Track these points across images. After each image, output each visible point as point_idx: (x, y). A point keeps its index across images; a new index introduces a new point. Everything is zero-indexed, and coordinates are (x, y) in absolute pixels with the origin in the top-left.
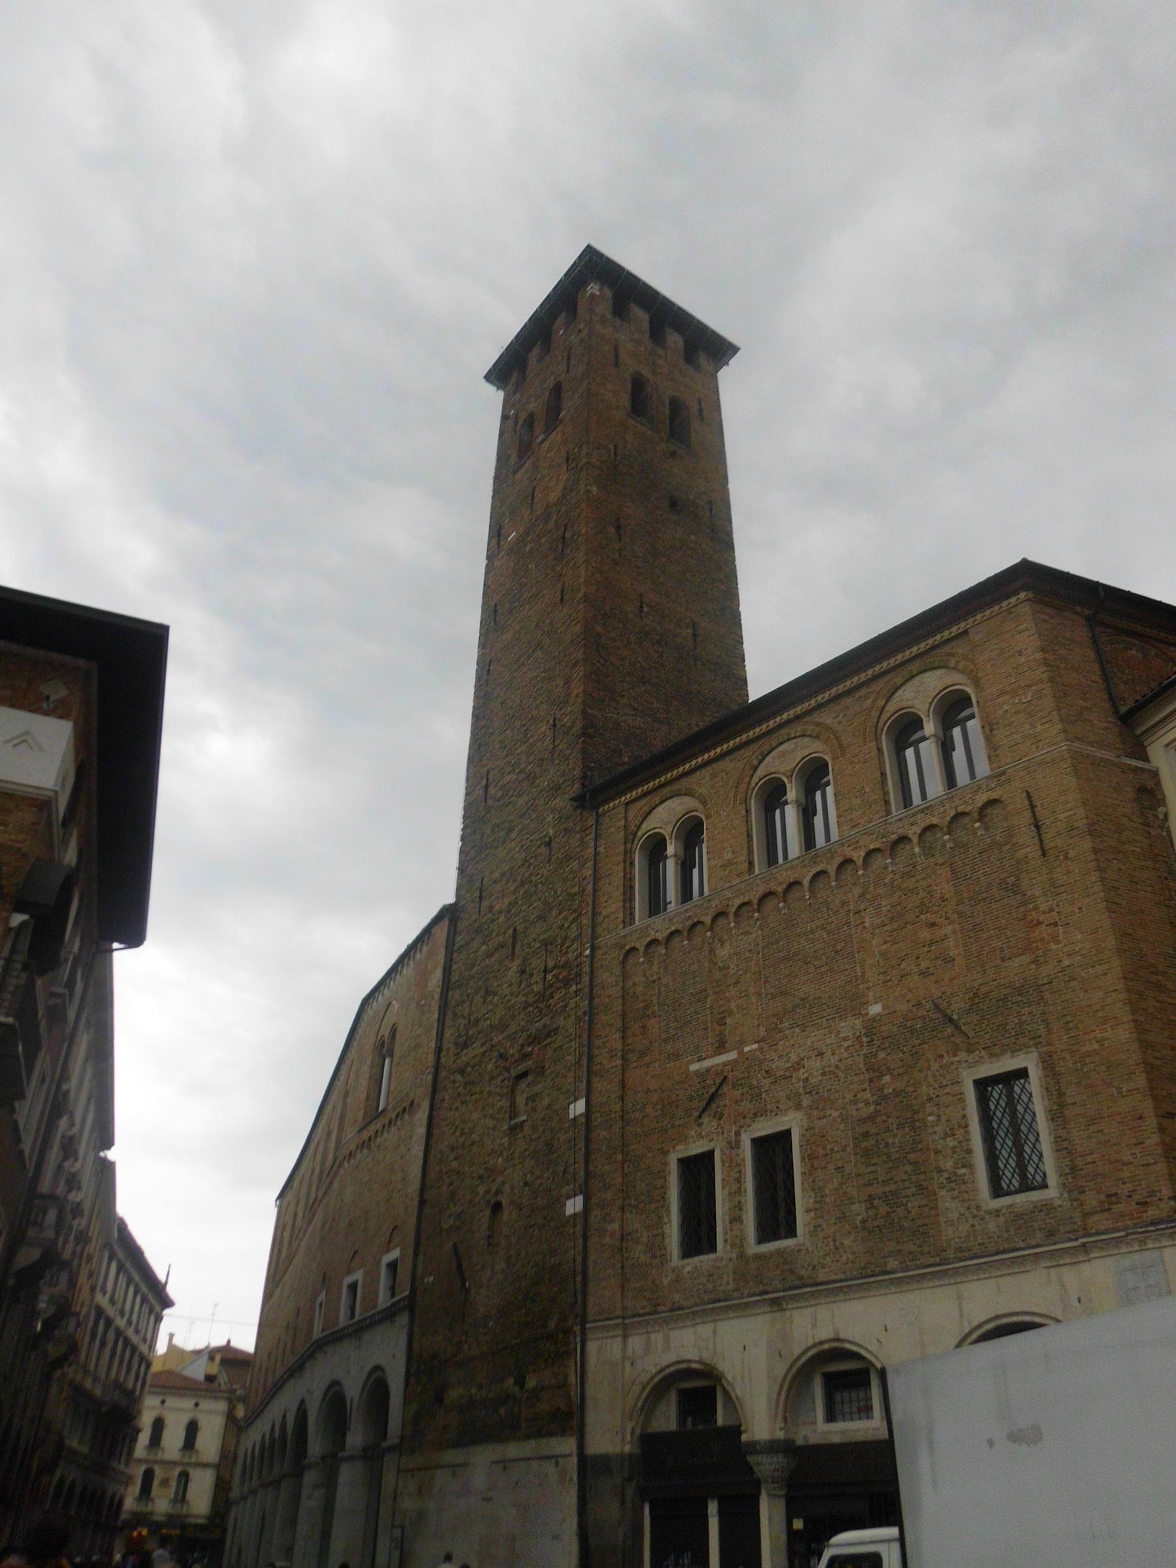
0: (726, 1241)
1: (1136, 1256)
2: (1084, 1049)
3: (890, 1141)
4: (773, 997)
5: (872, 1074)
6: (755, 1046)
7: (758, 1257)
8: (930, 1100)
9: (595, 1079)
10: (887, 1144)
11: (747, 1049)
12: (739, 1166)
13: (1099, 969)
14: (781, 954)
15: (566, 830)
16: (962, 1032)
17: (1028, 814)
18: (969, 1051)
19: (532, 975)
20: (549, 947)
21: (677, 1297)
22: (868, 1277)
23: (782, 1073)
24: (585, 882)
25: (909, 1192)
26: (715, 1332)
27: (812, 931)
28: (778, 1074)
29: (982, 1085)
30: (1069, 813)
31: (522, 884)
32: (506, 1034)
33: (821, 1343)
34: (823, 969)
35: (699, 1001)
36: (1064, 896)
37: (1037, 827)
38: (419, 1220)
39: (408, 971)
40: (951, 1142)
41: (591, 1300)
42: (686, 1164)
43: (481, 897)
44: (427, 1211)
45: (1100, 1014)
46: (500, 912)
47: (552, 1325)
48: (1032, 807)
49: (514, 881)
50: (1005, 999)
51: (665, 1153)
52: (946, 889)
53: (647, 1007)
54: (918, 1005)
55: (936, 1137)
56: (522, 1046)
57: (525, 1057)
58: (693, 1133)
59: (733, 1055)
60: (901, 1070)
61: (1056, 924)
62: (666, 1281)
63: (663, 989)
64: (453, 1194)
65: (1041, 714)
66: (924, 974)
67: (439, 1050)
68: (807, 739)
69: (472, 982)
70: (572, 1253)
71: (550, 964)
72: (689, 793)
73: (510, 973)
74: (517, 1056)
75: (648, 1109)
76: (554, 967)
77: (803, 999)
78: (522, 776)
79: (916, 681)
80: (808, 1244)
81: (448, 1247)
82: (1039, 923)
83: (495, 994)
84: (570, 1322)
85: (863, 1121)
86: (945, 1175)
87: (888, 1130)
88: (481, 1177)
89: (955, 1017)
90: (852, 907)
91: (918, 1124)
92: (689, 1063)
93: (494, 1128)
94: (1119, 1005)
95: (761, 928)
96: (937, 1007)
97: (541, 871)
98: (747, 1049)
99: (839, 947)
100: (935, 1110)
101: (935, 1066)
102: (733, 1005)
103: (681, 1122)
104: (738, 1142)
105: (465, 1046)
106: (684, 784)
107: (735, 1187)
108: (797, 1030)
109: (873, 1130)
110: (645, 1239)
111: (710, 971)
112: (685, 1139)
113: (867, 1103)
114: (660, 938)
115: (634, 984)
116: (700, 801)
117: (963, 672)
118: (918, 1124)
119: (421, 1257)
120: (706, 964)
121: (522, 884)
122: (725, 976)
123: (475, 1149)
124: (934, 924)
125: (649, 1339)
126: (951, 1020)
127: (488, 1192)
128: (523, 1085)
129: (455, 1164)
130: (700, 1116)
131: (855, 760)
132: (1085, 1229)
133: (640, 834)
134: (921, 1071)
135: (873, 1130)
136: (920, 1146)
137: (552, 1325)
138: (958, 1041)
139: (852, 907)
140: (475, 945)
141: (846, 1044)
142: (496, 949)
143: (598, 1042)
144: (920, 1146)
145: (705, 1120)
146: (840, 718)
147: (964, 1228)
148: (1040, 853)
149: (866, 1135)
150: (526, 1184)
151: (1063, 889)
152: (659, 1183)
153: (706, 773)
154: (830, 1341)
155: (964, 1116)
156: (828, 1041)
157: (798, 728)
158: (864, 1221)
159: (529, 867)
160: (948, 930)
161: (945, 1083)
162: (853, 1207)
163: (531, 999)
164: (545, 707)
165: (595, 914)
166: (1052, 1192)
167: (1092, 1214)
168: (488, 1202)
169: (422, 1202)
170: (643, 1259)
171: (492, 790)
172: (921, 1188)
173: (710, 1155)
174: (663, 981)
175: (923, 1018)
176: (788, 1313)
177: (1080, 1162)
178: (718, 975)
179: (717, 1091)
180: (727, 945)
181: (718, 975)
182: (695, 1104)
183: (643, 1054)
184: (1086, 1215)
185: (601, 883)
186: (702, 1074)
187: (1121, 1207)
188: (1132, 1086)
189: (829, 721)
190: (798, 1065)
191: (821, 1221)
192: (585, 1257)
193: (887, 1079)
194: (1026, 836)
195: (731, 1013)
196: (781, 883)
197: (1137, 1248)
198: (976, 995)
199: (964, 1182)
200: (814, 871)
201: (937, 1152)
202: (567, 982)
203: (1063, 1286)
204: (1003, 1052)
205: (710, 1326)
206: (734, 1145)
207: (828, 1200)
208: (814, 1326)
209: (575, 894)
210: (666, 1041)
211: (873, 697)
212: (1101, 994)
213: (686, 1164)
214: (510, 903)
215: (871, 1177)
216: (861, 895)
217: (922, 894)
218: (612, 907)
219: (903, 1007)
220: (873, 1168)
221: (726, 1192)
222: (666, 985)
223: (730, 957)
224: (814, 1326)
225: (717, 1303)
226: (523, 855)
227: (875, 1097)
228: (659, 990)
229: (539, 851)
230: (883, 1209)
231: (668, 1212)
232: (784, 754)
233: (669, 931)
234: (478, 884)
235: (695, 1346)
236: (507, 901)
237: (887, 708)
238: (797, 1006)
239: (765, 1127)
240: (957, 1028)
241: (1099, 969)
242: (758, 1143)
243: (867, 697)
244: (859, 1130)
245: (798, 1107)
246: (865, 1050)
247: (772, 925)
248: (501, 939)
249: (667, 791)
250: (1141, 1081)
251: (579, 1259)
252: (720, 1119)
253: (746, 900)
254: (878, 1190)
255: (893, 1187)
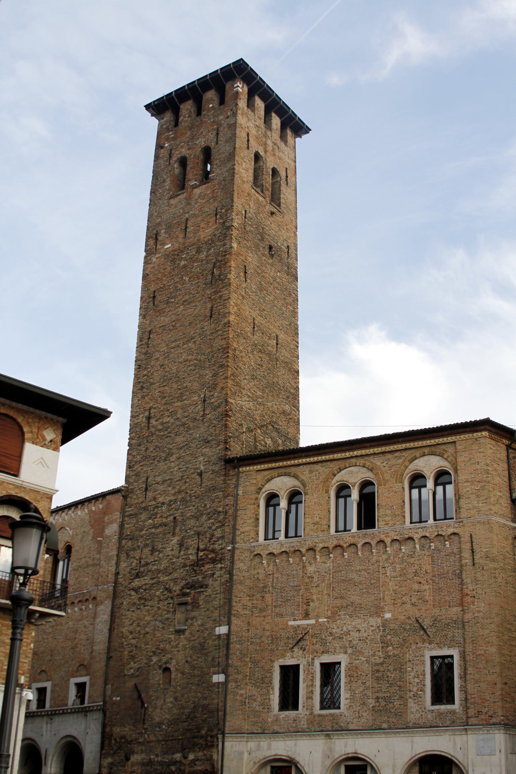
0: (304, 707)
1: (485, 735)
2: (478, 653)
3: (389, 675)
4: (336, 598)
5: (383, 645)
6: (325, 620)
7: (320, 715)
8: (410, 661)
9: (233, 618)
10: (388, 677)
11: (320, 620)
12: (313, 674)
13: (489, 621)
14: (343, 578)
15: (213, 471)
16: (428, 635)
17: (469, 545)
18: (430, 644)
19: (187, 549)
20: (201, 537)
21: (276, 728)
22: (373, 729)
23: (338, 635)
24: (227, 508)
25: (395, 698)
26: (295, 745)
27: (359, 571)
28: (336, 635)
29: (432, 658)
30: (487, 550)
31: (180, 492)
32: (170, 577)
33: (348, 754)
34: (364, 591)
35: (296, 590)
36: (480, 586)
37: (473, 552)
38: (107, 666)
39: (81, 513)
40: (417, 680)
41: (227, 724)
42: (284, 669)
43: (146, 490)
44: (112, 663)
45: (487, 640)
46: (163, 503)
47: (203, 732)
48: (472, 542)
49: (174, 488)
50: (448, 624)
51: (273, 661)
52: (429, 568)
53: (265, 587)
54: (409, 618)
55: (410, 677)
56: (183, 588)
57: (185, 595)
58: (288, 654)
59: (313, 622)
60: (398, 646)
61: (474, 597)
62: (269, 720)
63: (275, 580)
64: (133, 657)
65: (483, 498)
66: (413, 605)
67: (117, 574)
68: (365, 469)
69: (141, 540)
70: (216, 701)
71: (202, 547)
72: (296, 477)
73: (172, 543)
74: (178, 592)
75: (264, 639)
76: (205, 549)
77: (352, 603)
78: (178, 423)
79: (426, 458)
80: (346, 713)
81: (130, 684)
82: (467, 595)
83: (160, 552)
84: (215, 732)
85: (377, 664)
86: (413, 693)
87: (388, 670)
88: (154, 652)
89: (425, 627)
90: (381, 564)
91: (403, 670)
92: (288, 620)
93: (163, 628)
94: (495, 637)
95: (333, 562)
96: (417, 621)
97: (195, 489)
98: (320, 620)
99: (373, 582)
100: (411, 666)
101: (414, 647)
102: (314, 597)
103: (282, 648)
104: (313, 663)
105: (137, 576)
106: (293, 470)
107: (310, 683)
108: (348, 617)
109: (382, 669)
110: (259, 699)
111: (303, 577)
112: (283, 656)
113: (380, 657)
114: (275, 553)
115: (258, 573)
116: (302, 484)
117: (450, 463)
118: (403, 670)
119: (109, 686)
120: (301, 573)
121: (180, 492)
122: (311, 581)
123: (148, 636)
124: (420, 583)
125: (259, 745)
126: (423, 629)
127: (160, 661)
128: (183, 608)
129: (134, 641)
130: (293, 648)
131: (391, 490)
132: (467, 722)
133: (264, 490)
134: (407, 648)
135: (382, 669)
136: (403, 680)
137: (203, 732)
138: (425, 638)
139: (381, 564)
140: (143, 517)
141: (372, 628)
142: (160, 525)
143: (234, 599)
144: (403, 680)
145: (296, 649)
146: (384, 464)
147: (418, 715)
148: (472, 563)
149: (378, 671)
150: (187, 662)
151: (479, 582)
152: (268, 675)
153: (307, 468)
154: (353, 753)
155: (424, 671)
156: (363, 625)
157: (361, 461)
158: (373, 707)
159: (186, 483)
160: (426, 587)
161: (417, 655)
162: (369, 700)
163: (188, 562)
164: (196, 384)
165: (234, 528)
166: (457, 706)
167: (471, 717)
168: (160, 667)
169: (109, 658)
170: (258, 708)
171: (153, 422)
172: (401, 697)
173: (298, 666)
174: (275, 576)
175: (410, 624)
176: (333, 740)
177: (469, 697)
178: (307, 580)
179: (303, 637)
180: (314, 565)
181: (307, 580)
182: (291, 641)
183: (261, 610)
184: (468, 718)
185: (239, 512)
186: (295, 627)
187: (482, 717)
188: (494, 671)
189: (379, 464)
190: (348, 633)
191: (353, 704)
192: (225, 705)
193: (390, 648)
194: (466, 554)
195: (313, 601)
196: (346, 543)
197: (486, 732)
198: (435, 620)
199: (420, 697)
200: (364, 541)
201: (410, 683)
202: (214, 561)
203: (455, 742)
204: (445, 645)
205: (294, 742)
206: (311, 664)
207: (357, 695)
208: (345, 747)
209: (220, 512)
210: (275, 607)
211: (403, 458)
212: (488, 632)
213: (284, 669)
214: (171, 501)
215: (379, 689)
216: (387, 560)
217: (416, 567)
218: (244, 526)
219: (402, 618)
220: (380, 685)
221: (305, 684)
222: (277, 578)
223: (315, 572)
224: (345, 747)
225: (296, 731)
226: (180, 474)
227: (384, 656)
228: (273, 580)
229: (193, 476)
230: (383, 703)
231: (273, 689)
232: (352, 472)
233: (281, 551)
234: (144, 479)
235: (285, 749)
236: (168, 499)
237: (409, 467)
238: (349, 605)
239: (327, 659)
240: (426, 632)
241: (489, 621)
242: (322, 665)
243: (400, 457)
244: (375, 668)
245: (346, 653)
246: (381, 633)
247: (338, 562)
248: (164, 520)
249: (283, 470)
250: (497, 669)
251: (221, 704)
252: (304, 651)
253: (326, 546)
254: (380, 695)
255: (389, 695)
